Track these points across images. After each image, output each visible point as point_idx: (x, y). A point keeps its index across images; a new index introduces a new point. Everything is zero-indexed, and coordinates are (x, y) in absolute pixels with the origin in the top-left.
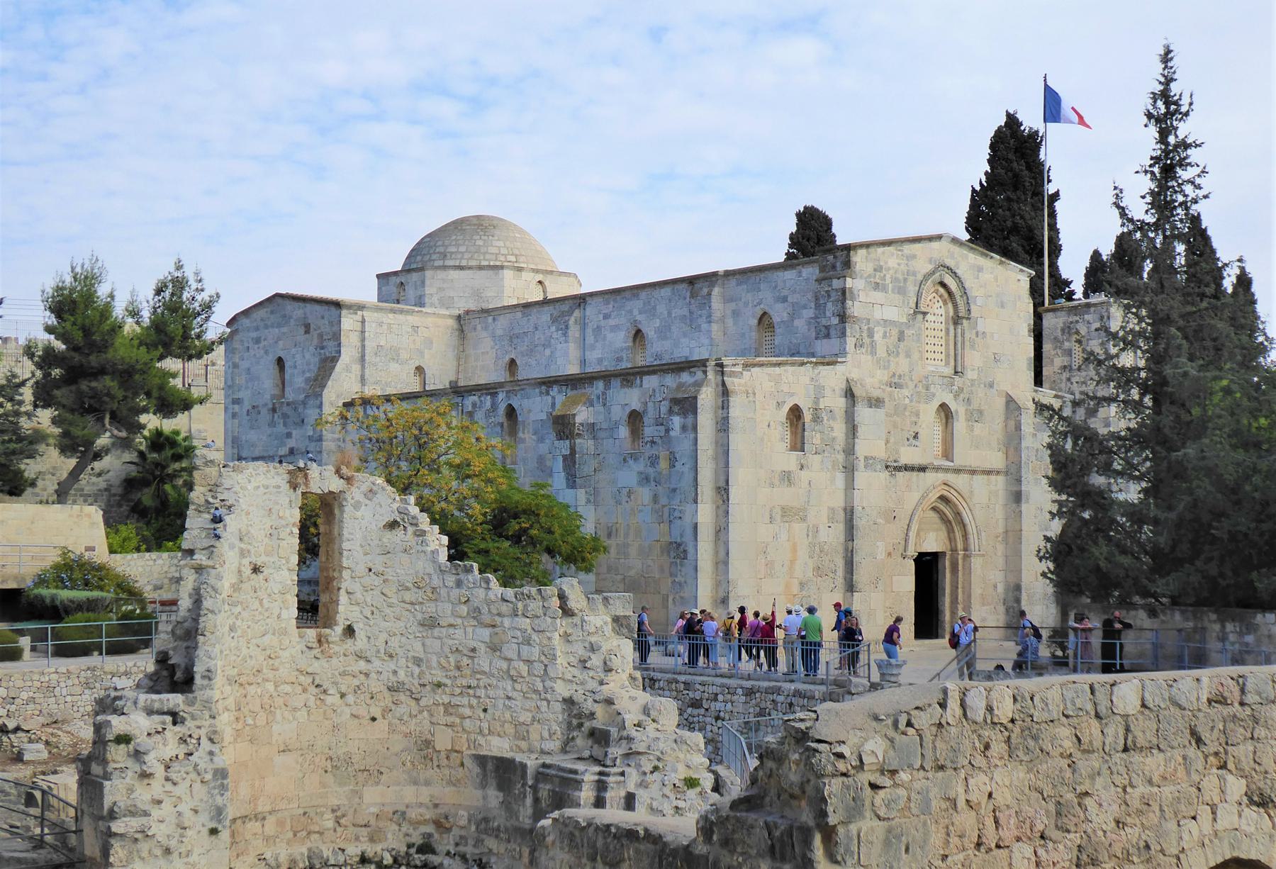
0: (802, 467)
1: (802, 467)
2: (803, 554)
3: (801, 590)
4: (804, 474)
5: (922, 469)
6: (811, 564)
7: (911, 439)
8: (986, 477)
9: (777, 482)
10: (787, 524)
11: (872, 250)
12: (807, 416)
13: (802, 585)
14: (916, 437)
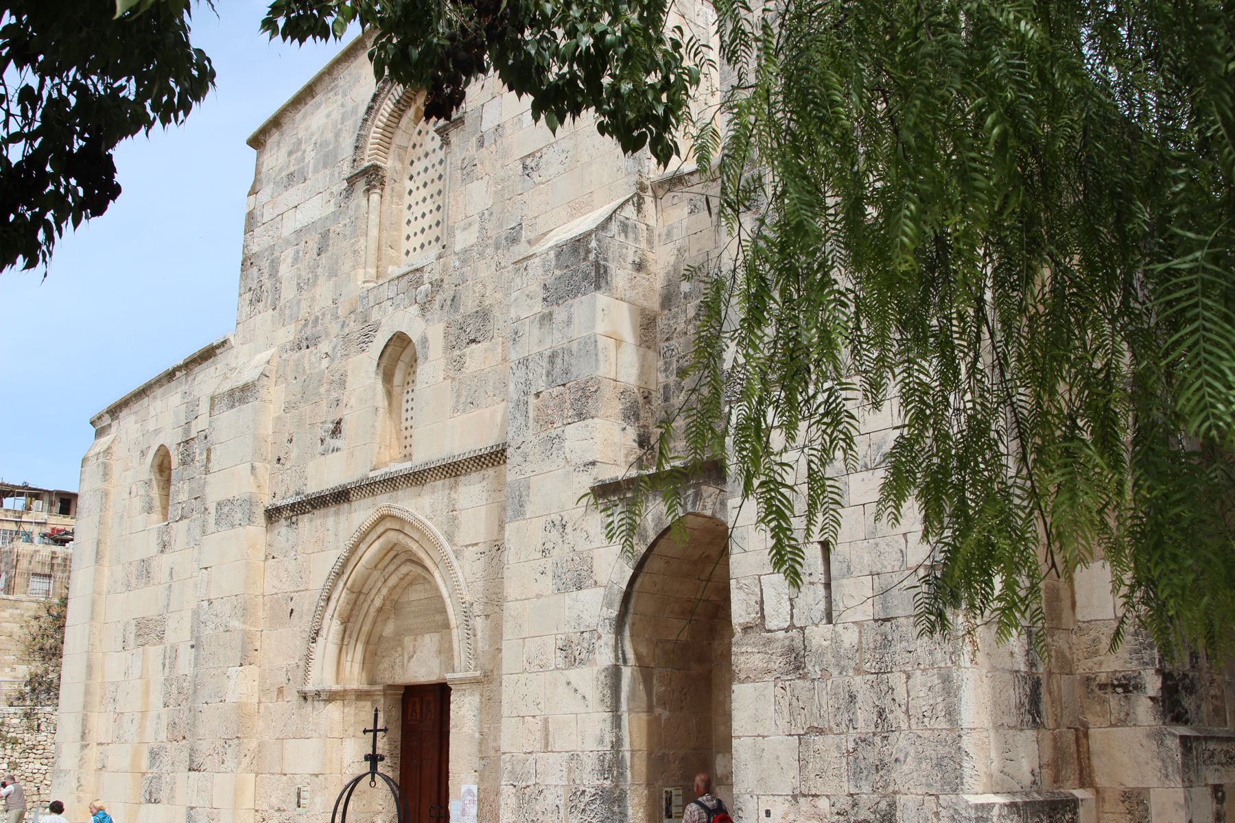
0: (164, 547)
1: (164, 547)
2: (156, 699)
3: (152, 765)
4: (166, 559)
5: (341, 496)
6: (165, 720)
7: (328, 439)
8: (490, 472)
9: (134, 581)
10: (141, 649)
11: (287, 126)
12: (175, 461)
13: (154, 755)
14: (336, 430)
